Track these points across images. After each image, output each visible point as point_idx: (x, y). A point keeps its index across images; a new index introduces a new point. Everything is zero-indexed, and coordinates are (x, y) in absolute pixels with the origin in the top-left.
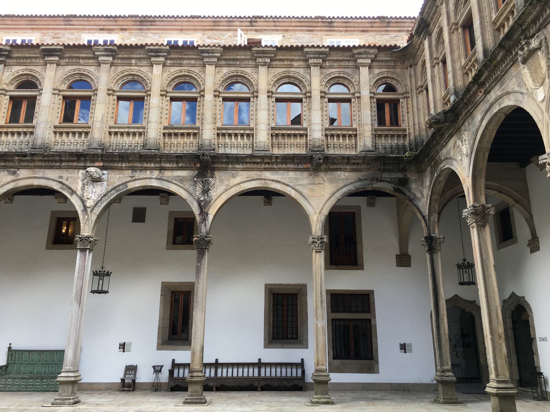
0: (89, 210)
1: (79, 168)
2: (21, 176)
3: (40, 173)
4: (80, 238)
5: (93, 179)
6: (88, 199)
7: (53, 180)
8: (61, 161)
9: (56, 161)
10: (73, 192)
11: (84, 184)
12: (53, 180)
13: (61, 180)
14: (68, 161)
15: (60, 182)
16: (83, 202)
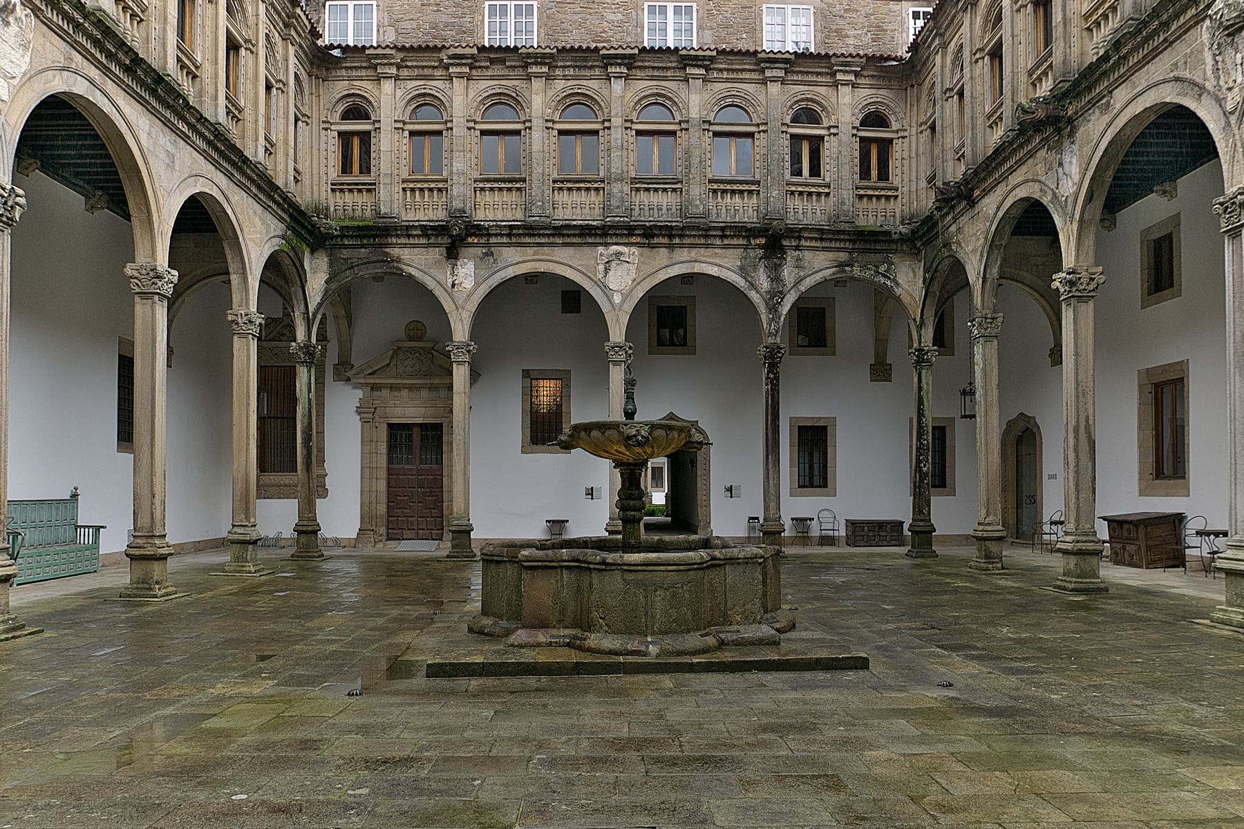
0: (1233, 119)
1: (1199, 20)
2: (1118, 106)
3: (1142, 79)
4: (1221, 204)
5: (1227, 28)
6: (1230, 89)
7: (1165, 81)
8: (1165, 25)
9: (1156, 33)
10: (1200, 90)
11: (1215, 55)
12: (1165, 81)
13: (1176, 73)
14: (1177, 16)
15: (1177, 79)
16: (1220, 101)
